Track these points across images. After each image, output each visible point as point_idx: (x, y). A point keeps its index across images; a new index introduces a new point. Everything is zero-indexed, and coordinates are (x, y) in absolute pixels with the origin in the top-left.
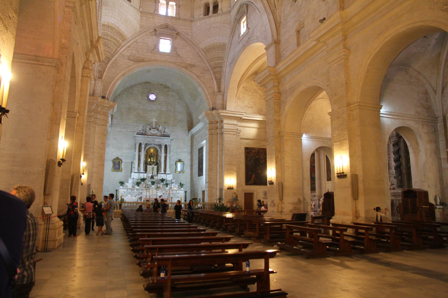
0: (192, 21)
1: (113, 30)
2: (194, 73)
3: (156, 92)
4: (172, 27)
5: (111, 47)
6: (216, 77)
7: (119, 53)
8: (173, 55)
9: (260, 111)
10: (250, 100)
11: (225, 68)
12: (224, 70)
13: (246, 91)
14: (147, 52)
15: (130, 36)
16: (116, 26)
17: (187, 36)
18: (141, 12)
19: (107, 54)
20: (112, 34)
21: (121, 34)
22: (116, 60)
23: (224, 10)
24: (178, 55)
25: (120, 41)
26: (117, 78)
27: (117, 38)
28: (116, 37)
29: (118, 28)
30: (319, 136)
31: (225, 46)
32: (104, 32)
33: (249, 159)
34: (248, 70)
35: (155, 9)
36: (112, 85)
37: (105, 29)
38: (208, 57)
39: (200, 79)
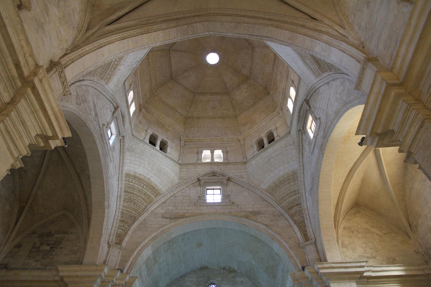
0: (245, 163)
1: (142, 182)
2: (260, 223)
3: (216, 280)
4: (220, 173)
5: (139, 203)
6: (295, 221)
7: (150, 211)
8: (226, 204)
9: (392, 260)
10: (365, 245)
11: (305, 203)
12: (305, 207)
13: (351, 232)
14: (188, 206)
15: (165, 190)
16: (145, 178)
17: (242, 179)
18: (180, 164)
19: (132, 213)
20: (140, 187)
21: (153, 187)
22: (145, 220)
23: (282, 135)
24: (233, 203)
25: (152, 195)
26: (144, 243)
27: (148, 192)
28: (146, 191)
29: (149, 179)
31: (296, 174)
32: (129, 184)
34: (342, 195)
35: (197, 159)
36: (135, 253)
37: (131, 181)
38: (276, 198)
39: (271, 229)
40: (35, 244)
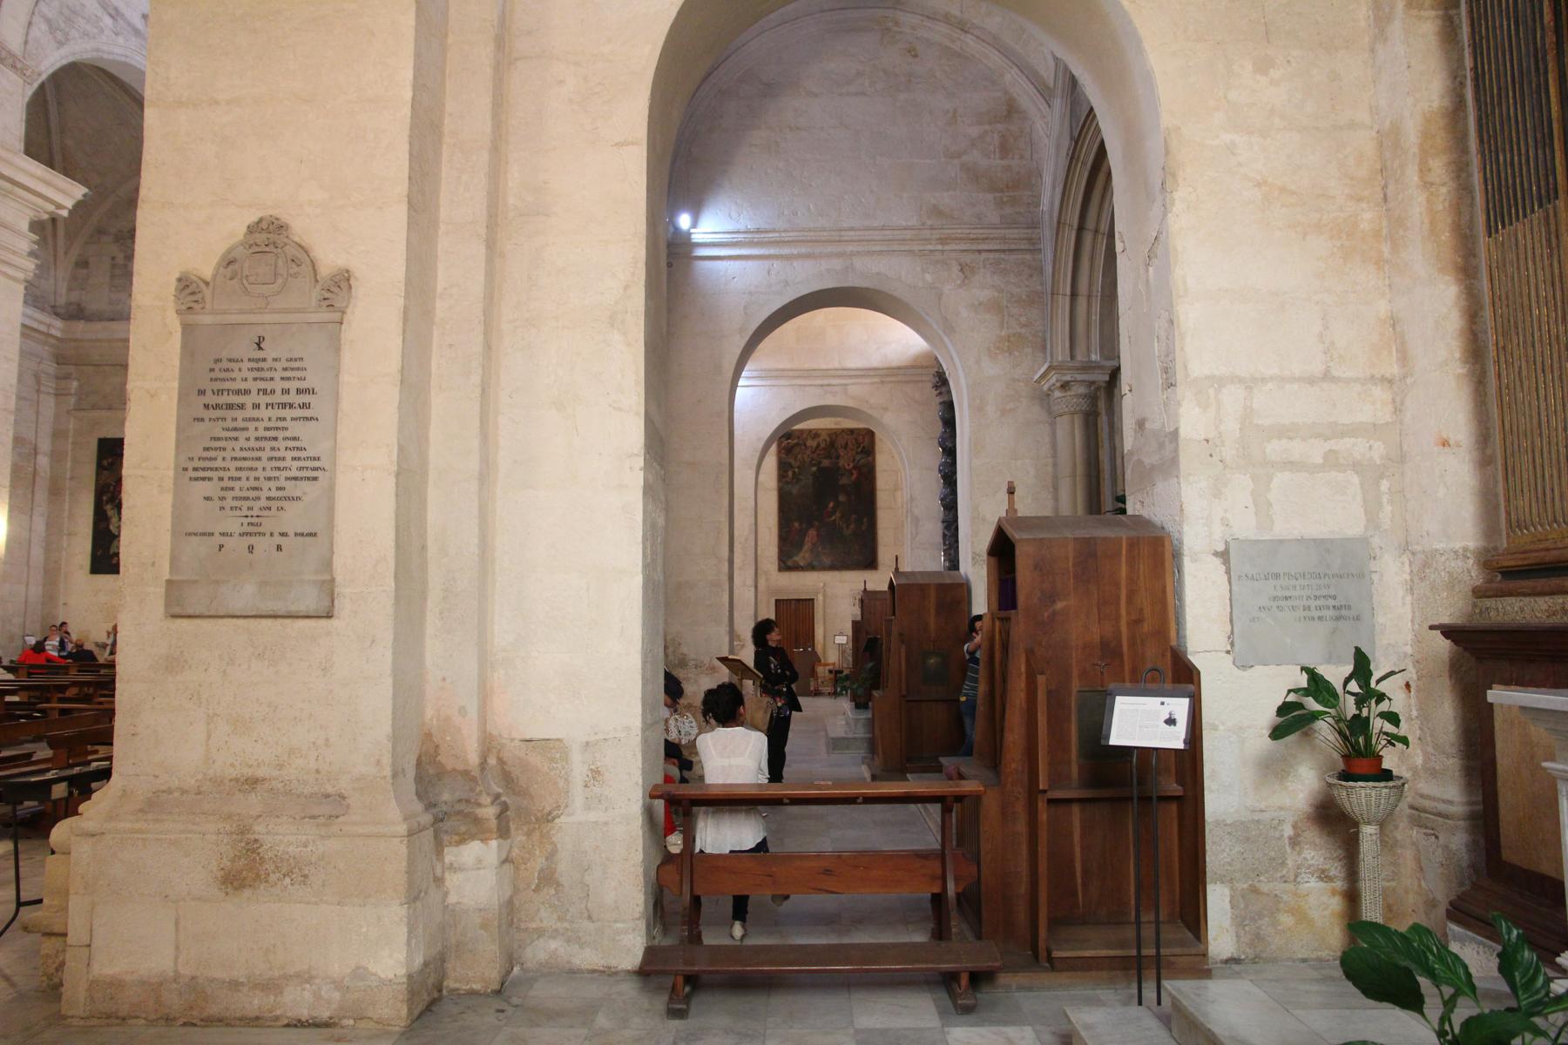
30: (806, 366)
33: (794, 472)
40: (113, 258)
